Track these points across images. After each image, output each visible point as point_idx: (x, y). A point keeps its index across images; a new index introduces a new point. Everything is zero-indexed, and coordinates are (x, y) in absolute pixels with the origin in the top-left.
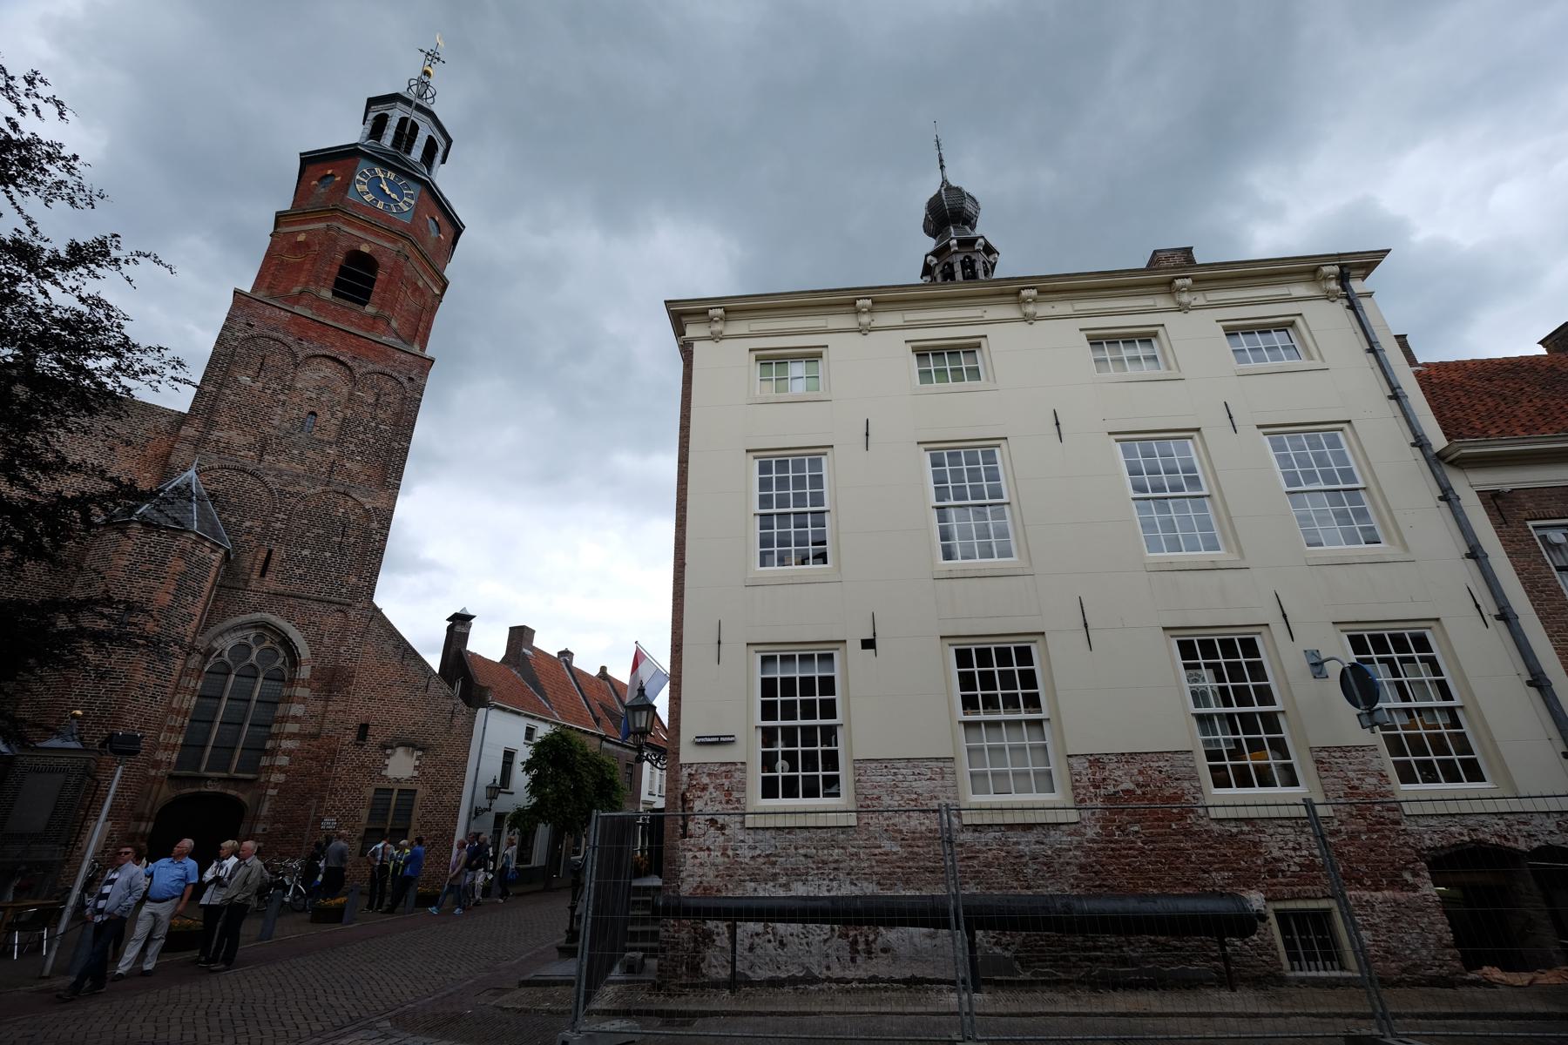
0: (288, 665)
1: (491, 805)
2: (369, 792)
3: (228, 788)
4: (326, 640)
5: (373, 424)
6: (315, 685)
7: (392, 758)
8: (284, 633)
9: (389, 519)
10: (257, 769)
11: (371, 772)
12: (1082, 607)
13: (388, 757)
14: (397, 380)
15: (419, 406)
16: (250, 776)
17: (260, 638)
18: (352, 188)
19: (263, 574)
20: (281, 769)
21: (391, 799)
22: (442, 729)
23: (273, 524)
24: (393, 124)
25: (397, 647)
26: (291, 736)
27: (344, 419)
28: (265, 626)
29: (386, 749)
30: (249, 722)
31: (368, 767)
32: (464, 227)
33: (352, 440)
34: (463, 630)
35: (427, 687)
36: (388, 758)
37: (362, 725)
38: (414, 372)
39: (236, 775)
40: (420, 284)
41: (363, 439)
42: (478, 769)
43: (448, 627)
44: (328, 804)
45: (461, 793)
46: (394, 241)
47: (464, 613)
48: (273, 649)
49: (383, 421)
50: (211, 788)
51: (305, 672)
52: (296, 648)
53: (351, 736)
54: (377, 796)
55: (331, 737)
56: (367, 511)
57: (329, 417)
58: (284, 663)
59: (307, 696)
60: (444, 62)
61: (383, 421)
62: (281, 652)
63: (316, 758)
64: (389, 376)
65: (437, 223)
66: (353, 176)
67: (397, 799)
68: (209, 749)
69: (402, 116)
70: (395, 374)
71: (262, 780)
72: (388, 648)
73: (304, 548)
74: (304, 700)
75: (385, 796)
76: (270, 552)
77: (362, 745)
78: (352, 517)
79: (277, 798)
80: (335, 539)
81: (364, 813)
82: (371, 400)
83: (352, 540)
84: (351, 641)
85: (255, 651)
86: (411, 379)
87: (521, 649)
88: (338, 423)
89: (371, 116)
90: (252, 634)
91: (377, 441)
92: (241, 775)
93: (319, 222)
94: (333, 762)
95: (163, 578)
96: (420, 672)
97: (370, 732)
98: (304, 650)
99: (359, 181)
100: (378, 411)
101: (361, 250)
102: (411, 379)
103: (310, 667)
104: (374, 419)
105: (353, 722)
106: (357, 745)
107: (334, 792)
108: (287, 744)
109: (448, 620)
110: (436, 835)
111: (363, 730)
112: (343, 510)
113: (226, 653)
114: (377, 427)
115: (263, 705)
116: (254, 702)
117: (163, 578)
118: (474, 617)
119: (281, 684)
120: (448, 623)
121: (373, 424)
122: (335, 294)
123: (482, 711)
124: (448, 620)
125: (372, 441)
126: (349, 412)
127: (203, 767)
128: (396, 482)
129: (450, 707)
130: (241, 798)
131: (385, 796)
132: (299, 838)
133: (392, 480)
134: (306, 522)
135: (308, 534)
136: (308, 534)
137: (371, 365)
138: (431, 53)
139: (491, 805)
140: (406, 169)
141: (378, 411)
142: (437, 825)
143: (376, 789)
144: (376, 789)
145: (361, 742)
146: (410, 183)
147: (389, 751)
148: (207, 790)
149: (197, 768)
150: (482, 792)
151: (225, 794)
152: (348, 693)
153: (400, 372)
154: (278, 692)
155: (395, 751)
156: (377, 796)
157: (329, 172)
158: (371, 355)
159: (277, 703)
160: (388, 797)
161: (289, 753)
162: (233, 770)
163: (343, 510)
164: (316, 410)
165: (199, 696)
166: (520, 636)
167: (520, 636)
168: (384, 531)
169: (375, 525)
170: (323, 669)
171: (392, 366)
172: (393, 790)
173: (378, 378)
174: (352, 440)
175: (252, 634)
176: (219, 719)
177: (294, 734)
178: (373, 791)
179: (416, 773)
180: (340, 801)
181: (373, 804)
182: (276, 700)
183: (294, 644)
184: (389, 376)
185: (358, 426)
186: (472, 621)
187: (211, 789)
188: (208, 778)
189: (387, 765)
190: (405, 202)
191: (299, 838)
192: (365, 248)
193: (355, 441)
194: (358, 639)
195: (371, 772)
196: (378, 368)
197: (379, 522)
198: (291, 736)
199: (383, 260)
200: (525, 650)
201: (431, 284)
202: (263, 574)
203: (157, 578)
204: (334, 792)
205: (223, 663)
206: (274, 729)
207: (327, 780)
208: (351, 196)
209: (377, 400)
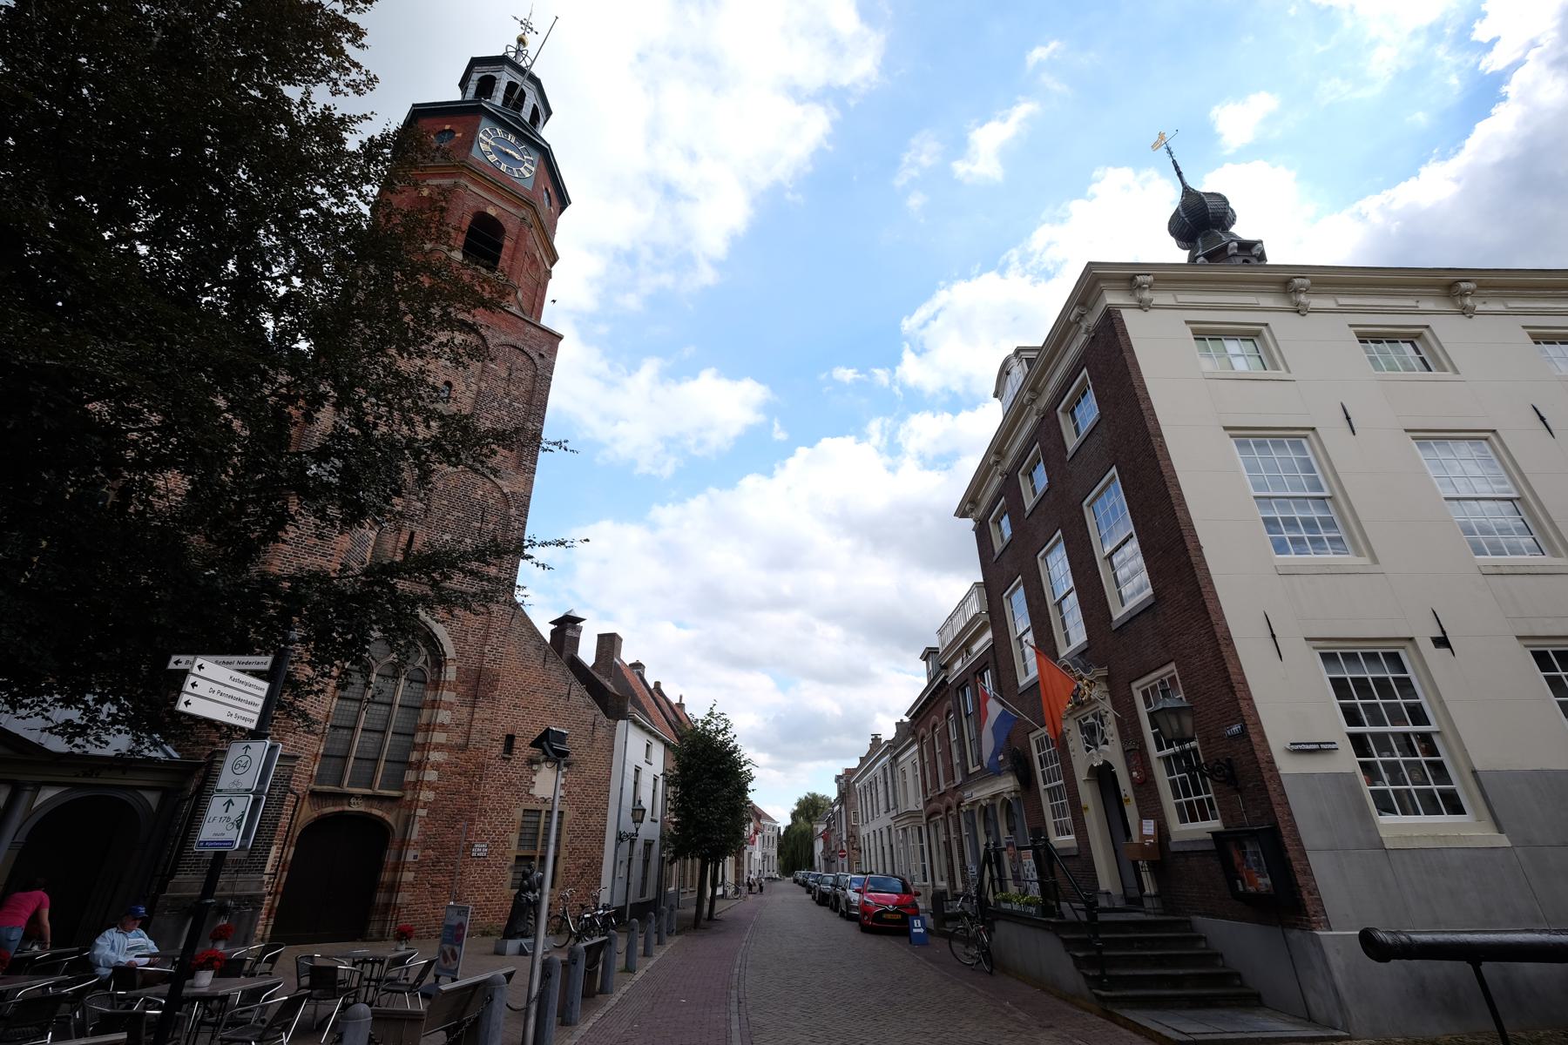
1: (637, 829)
2: (518, 814)
3: (371, 807)
4: (469, 637)
5: (507, 401)
6: (460, 689)
7: (538, 775)
8: (428, 627)
9: (526, 506)
10: (401, 786)
11: (519, 791)
12: (1436, 615)
13: (535, 773)
14: (528, 355)
15: (550, 386)
16: (395, 793)
18: (476, 145)
20: (431, 786)
21: (539, 822)
22: (584, 743)
23: (414, 503)
24: (502, 86)
25: (538, 649)
26: (439, 747)
27: (479, 392)
29: (532, 764)
30: (391, 730)
31: (515, 785)
32: (570, 203)
33: (488, 416)
34: (574, 635)
35: (569, 694)
36: (535, 775)
37: (508, 736)
38: (545, 348)
39: (380, 791)
40: (538, 256)
41: (497, 416)
42: (622, 789)
43: (552, 631)
44: (477, 827)
45: (605, 815)
46: (518, 207)
47: (570, 614)
49: (516, 399)
50: (357, 807)
51: (451, 673)
52: (441, 645)
53: (498, 749)
54: (526, 819)
55: (478, 749)
56: (505, 495)
57: (464, 388)
58: (426, 662)
59: (453, 701)
60: (537, 33)
61: (516, 399)
63: (464, 774)
64: (520, 349)
65: (549, 194)
66: (475, 133)
67: (545, 823)
68: (352, 759)
70: (526, 349)
71: (408, 798)
72: (530, 649)
73: (444, 532)
74: (450, 706)
75: (534, 819)
76: (412, 535)
77: (509, 759)
78: (491, 501)
79: (427, 820)
80: (475, 524)
81: (514, 838)
82: (504, 375)
83: (491, 526)
84: (495, 640)
86: (541, 356)
87: (613, 659)
88: (473, 396)
89: (475, 77)
91: (512, 419)
92: (386, 792)
93: (442, 178)
94: (481, 779)
95: (330, 555)
96: (561, 678)
97: (516, 744)
98: (449, 649)
99: (482, 141)
100: (511, 387)
102: (541, 356)
103: (455, 667)
104: (507, 395)
105: (500, 735)
106: (504, 758)
107: (483, 812)
108: (435, 756)
110: (584, 864)
112: (482, 493)
114: (511, 404)
115: (404, 709)
116: (397, 706)
117: (330, 555)
118: (583, 620)
119: (422, 686)
120: (553, 627)
121: (507, 401)
123: (621, 724)
125: (506, 418)
126: (483, 385)
127: (346, 783)
128: (532, 465)
129: (590, 719)
130: (387, 819)
131: (534, 819)
132: (450, 868)
133: (527, 463)
134: (446, 502)
135: (448, 517)
136: (448, 517)
137: (503, 337)
138: (525, 22)
139: (637, 829)
140: (527, 133)
141: (511, 387)
142: (585, 852)
143: (525, 810)
144: (525, 810)
145: (506, 756)
146: (530, 150)
147: (535, 767)
148: (350, 809)
149: (340, 784)
150: (627, 815)
151: (371, 814)
152: (494, 699)
153: (530, 347)
154: (420, 695)
155: (541, 767)
156: (526, 819)
157: (447, 127)
158: (503, 325)
159: (419, 708)
160: (536, 819)
161: (437, 766)
162: (377, 785)
163: (482, 493)
164: (451, 379)
165: (339, 698)
166: (609, 643)
167: (609, 643)
168: (522, 519)
169: (513, 511)
170: (468, 670)
171: (524, 340)
172: (540, 811)
173: (510, 352)
174: (488, 416)
176: (361, 726)
177: (442, 745)
178: (522, 812)
180: (490, 824)
181: (522, 828)
182: (418, 704)
183: (438, 640)
184: (520, 349)
185: (493, 401)
186: (581, 624)
187: (355, 808)
188: (352, 795)
189: (534, 783)
190: (526, 168)
191: (450, 868)
192: (491, 211)
193: (491, 417)
194: (501, 638)
195: (519, 791)
196: (511, 340)
197: (517, 508)
198: (439, 747)
199: (510, 226)
200: (616, 660)
201: (545, 259)
203: (324, 555)
204: (483, 812)
206: (419, 738)
207: (476, 799)
208: (475, 153)
209: (510, 375)
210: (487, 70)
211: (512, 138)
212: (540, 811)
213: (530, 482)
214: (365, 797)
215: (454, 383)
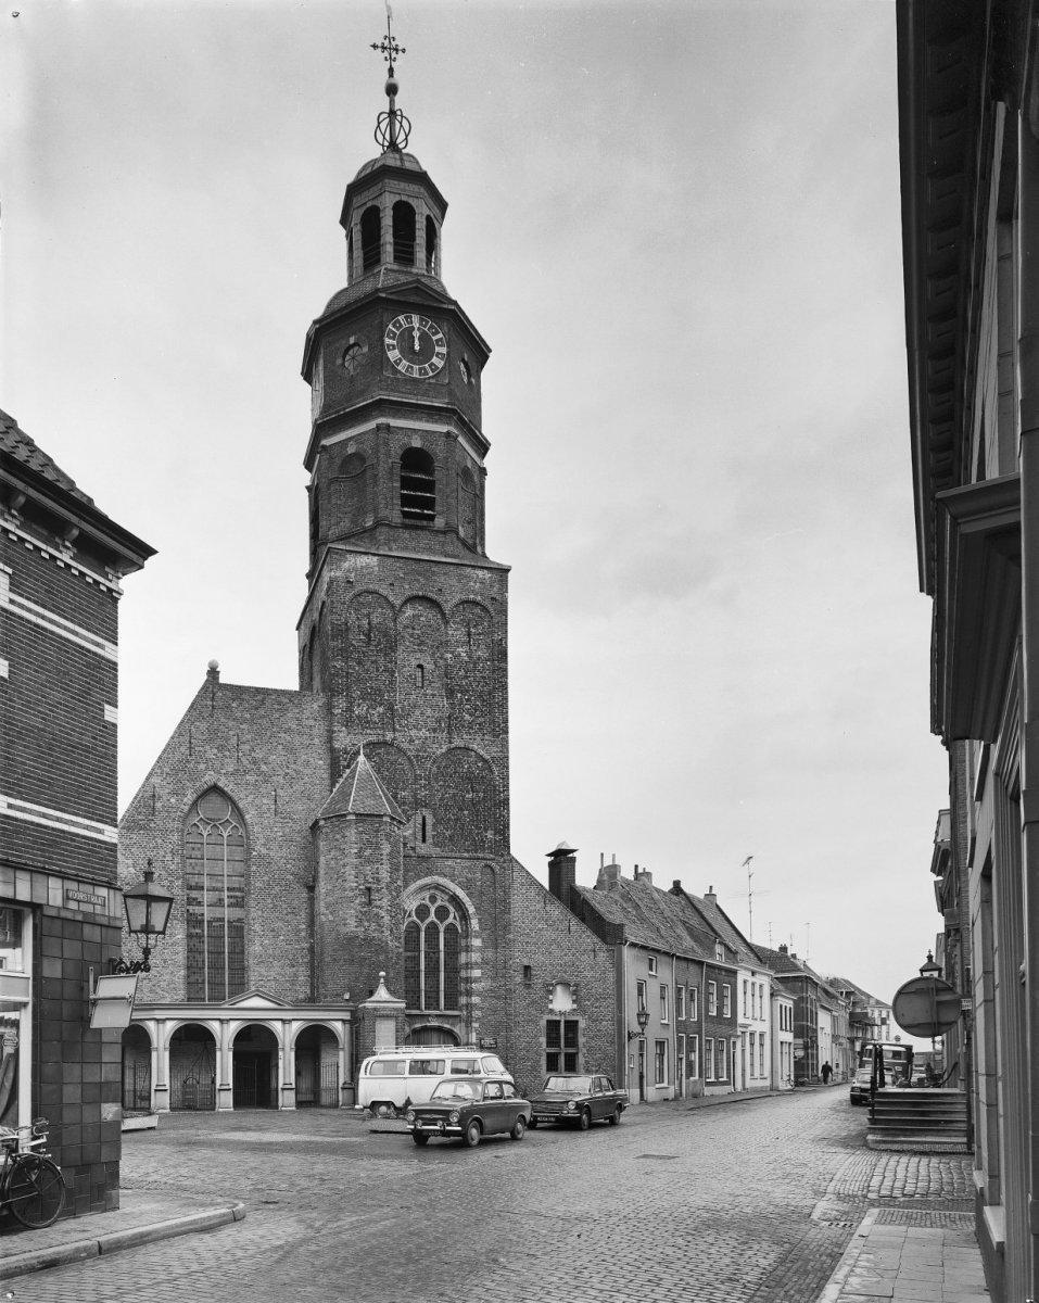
17: (433, 899)
19: (424, 841)
27: (447, 666)
28: (437, 887)
58: (455, 918)
62: (452, 909)
76: (424, 818)
83: (481, 795)
85: (433, 910)
90: (427, 895)
124: (549, 855)
175: (427, 895)
186: (575, 854)
202: (424, 841)
205: (413, 922)
215: (425, 665)
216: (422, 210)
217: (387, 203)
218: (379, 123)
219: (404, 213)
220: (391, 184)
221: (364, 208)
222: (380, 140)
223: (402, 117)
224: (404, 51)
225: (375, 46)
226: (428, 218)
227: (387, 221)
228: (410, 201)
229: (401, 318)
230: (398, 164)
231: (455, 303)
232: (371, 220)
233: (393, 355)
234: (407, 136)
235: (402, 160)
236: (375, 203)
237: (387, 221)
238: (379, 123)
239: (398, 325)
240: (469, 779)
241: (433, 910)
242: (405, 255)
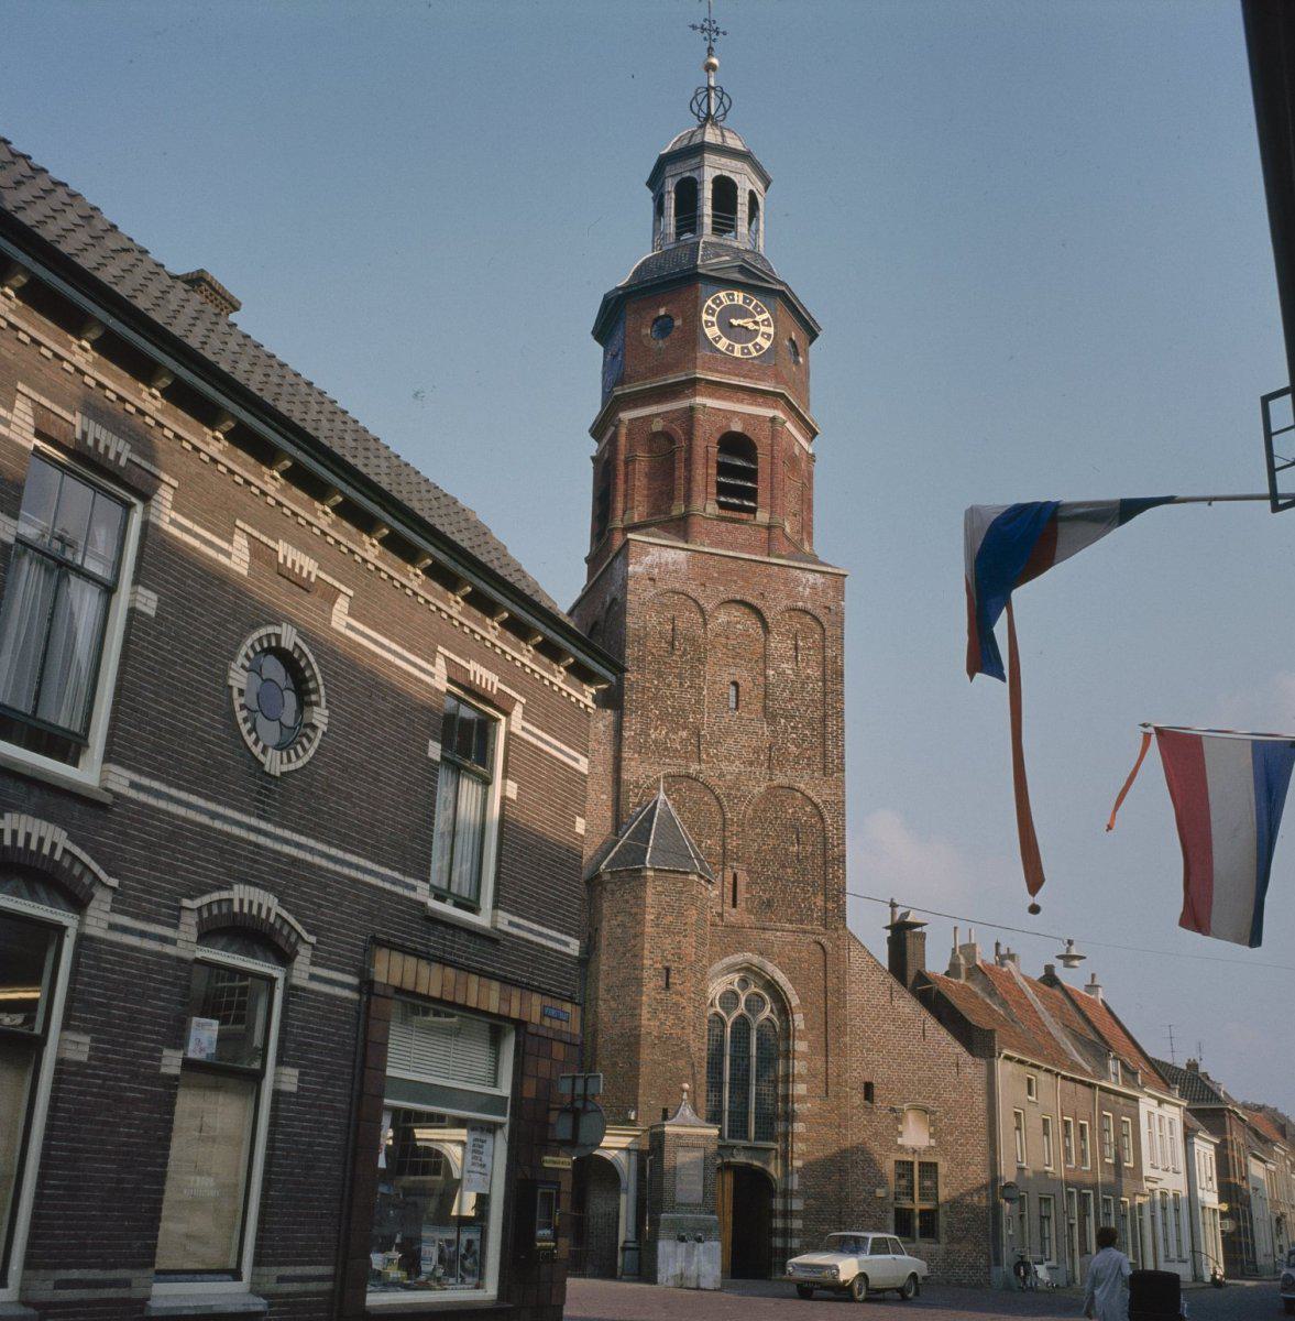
0: (776, 1012)
17: (744, 983)
19: (734, 906)
48: (757, 995)
58: (772, 1011)
69: (714, 175)
76: (735, 876)
83: (809, 849)
85: (743, 999)
89: (670, 185)
90: (736, 977)
97: (876, 1091)
101: (734, 429)
109: (887, 928)
111: (868, 1090)
113: (717, 1002)
122: (722, 506)
144: (896, 1161)
151: (752, 1165)
164: (736, 678)
179: (933, 1142)
186: (925, 929)
192: (737, 427)
202: (734, 906)
205: (716, 1014)
210: (683, 170)
211: (739, 297)
212: (912, 1163)
213: (841, 784)
214: (745, 1148)
215: (740, 682)
216: (746, 183)
217: (709, 175)
218: (697, 95)
219: (725, 189)
220: (709, 158)
221: (679, 178)
222: (696, 109)
223: (723, 93)
224: (724, 33)
225: (694, 27)
226: (752, 194)
227: (707, 193)
228: (732, 176)
229: (722, 295)
230: (719, 141)
231: (781, 283)
232: (688, 193)
233: (712, 332)
234: (726, 112)
235: (723, 136)
236: (695, 175)
237: (707, 193)
238: (697, 95)
239: (718, 301)
240: (793, 827)
241: (743, 999)
242: (725, 222)
